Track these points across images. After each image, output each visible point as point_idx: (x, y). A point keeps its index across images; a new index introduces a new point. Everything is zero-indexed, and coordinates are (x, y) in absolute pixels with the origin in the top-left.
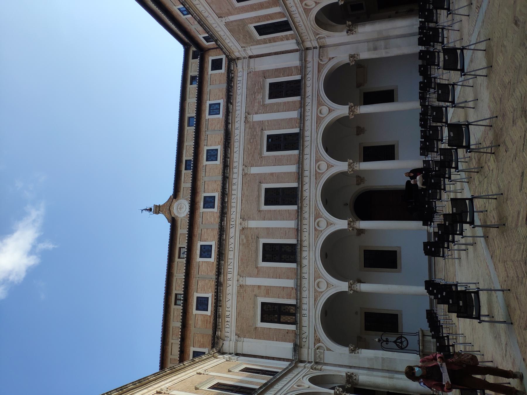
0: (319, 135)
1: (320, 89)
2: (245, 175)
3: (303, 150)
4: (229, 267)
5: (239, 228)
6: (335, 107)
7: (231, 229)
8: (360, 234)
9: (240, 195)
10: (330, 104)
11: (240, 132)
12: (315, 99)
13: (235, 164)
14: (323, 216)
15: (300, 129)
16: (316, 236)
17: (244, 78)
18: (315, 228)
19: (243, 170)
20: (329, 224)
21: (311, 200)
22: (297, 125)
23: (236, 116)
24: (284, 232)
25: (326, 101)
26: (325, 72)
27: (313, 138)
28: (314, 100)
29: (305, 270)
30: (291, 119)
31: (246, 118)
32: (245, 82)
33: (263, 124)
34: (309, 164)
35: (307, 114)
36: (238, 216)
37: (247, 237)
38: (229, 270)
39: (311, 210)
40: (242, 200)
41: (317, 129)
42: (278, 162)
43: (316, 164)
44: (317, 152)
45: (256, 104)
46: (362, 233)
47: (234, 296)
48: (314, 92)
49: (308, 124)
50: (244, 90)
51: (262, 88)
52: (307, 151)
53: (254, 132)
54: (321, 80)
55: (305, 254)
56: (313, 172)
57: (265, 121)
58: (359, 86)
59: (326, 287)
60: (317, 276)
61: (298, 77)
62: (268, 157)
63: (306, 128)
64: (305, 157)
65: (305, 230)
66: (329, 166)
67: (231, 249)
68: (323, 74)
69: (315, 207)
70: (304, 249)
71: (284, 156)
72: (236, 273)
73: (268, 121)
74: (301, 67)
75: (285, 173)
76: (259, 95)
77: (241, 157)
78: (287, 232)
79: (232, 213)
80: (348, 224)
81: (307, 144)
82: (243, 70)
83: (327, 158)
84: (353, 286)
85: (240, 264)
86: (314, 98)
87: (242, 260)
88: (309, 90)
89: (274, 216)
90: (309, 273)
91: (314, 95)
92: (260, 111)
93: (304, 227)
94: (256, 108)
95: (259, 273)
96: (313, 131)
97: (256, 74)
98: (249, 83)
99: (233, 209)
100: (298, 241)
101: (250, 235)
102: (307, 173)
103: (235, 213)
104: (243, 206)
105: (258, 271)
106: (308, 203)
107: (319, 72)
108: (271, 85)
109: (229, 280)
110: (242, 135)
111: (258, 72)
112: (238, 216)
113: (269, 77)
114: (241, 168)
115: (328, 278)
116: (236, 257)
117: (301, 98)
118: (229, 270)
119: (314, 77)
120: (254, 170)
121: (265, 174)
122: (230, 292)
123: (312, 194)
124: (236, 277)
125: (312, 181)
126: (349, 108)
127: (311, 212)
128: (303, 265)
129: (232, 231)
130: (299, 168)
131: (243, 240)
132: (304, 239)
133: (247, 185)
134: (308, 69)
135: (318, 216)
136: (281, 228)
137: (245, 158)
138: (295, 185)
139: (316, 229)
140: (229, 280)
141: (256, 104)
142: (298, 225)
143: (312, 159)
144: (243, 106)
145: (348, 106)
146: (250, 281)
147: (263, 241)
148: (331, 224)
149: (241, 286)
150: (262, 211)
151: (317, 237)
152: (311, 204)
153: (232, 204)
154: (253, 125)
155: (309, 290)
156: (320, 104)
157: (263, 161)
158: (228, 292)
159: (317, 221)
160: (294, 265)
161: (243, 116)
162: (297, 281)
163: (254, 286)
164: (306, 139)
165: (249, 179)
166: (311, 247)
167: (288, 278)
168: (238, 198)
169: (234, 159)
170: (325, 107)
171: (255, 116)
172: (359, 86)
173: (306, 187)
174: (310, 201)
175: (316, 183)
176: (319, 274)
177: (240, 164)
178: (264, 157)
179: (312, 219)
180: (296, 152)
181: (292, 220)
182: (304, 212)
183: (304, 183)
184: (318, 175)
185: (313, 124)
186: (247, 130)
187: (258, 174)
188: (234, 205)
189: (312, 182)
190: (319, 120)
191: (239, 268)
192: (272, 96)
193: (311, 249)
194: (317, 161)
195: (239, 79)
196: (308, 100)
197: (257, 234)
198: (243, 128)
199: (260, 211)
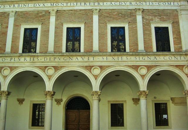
0: (122, 67)
1: (162, 68)
2: (91, 11)
3: (110, 55)
4: (23, 5)
5: (50, 9)
6: (146, 80)
7: (50, 4)
8: (56, 101)
9: (76, 8)
10: (148, 75)
11: (127, 6)
12: (154, 64)
13: (101, 4)
14: (56, 72)
15: (128, 53)
16: (41, 68)
17: (172, 7)
18: (47, 67)
19: (96, 10)
20: (50, 77)
21: (69, 63)
22: (132, 50)
23: (142, 2)
24: (45, 44)
25: (151, 72)
26: (177, 71)
27: (120, 63)
28: (152, 63)
29: (17, 59)
30: (137, 45)
31: (139, 9)
32: (169, 8)
33: (134, 23)
34: (100, 60)
35: (141, 57)
36: (60, 9)
37: (43, 16)
38: (21, 5)
39: (61, 63)
40: (72, 10)
41: (128, 66)
42: (102, 36)
43: (98, 66)
44: (109, 66)
45: (151, 17)
46: (57, 103)
47: (3, 10)
48: (159, 63)
49: (133, 58)
50: (163, 7)
51: (164, 21)
52: (110, 58)
53: (128, 16)
54: (169, 68)
55: (28, 59)
56: (91, 64)
57: (136, 25)
58: (172, 99)
59: (4, 75)
60: (12, 69)
61: (172, 49)
62: (106, 29)
63: (129, 57)
64: (105, 58)
65: (46, 59)
66: (96, 77)
67: (35, 5)
68: (174, 69)
69: (64, 67)
70: (32, 58)
71: (107, 41)
72: (18, 10)
73: (136, 27)
74: (181, 51)
75: (92, 42)
76: (158, 19)
77: (107, 7)
78: (45, 46)
79: (63, 3)
80: (49, 92)
81: (116, 58)
82: (180, 6)
83: (103, 74)
84: (5, 94)
85: (24, 12)
86: (154, 63)
87: (27, 13)
88: (162, 58)
89: (58, 35)
90: (14, 63)
91: (157, 63)
92: (145, 21)
93: (48, 58)
94: (147, 17)
95: (17, 26)
96: (126, 63)
97: (177, 16)
98: (169, 11)
99: (65, 4)
100: (37, 53)
101: (44, 18)
102: (91, 59)
103: (62, 5)
104: (67, 11)
105: (17, 26)
106: (67, 61)
107: (177, 66)
108: (167, 28)
109: (14, 6)
110: (125, 8)
111: (178, 18)
112: (59, 8)
113: (173, 27)
114: (98, 8)
115: (10, 76)
116: (29, 9)
117: (154, 53)
118: (21, 5)
119: (172, 63)
120: (96, 18)
121: (92, 27)
122: (6, 7)
123: (75, 64)
124: (14, 10)
125: (85, 63)
126: (144, 91)
127: (59, 63)
128: (20, 58)
129: (49, 5)
130: (95, 53)
131: (41, 13)
132: (39, 58)
133: (84, 13)
134: (179, 57)
135: (56, 68)
136: (48, 41)
137: (106, 11)
138: (82, 50)
139: (46, 67)
140: (14, 6)
141: (151, 17)
142: (49, 53)
143: (103, 63)
144: (149, 7)
145: (146, 90)
146: (11, 21)
147: (39, 27)
148: (49, 79)
149: (9, 15)
150: (63, 26)
151: (40, 68)
152: (66, 63)
153: (70, 3)
154: (133, 16)
155: (2, 63)
156: (149, 68)
157: (103, 25)
158: (6, 6)
159: (53, 68)
160: (20, 51)
161: (141, 7)
162: (8, 54)
163: (8, 23)
164: (120, 58)
165: (89, 14)
166: (33, 64)
167: (12, 47)
168: (73, 8)
169: (106, 3)
170: (147, 71)
171: (141, 17)
172: (172, 99)
173: (80, 59)
174: (68, 62)
175: (83, 67)
176: (13, 70)
177: (101, 7)
178: (106, 25)
179: (54, 64)
180: (109, 49)
181: (54, 49)
182: (60, 58)
183: (83, 57)
184: (89, 68)
185: (132, 63)
186: (129, 11)
187: (92, 21)
188: (69, 4)
189: (83, 63)
190: (136, 68)
191: (21, 12)
192: (157, 29)
193: (31, 64)
194: (101, 67)
195: (172, 3)
196: (152, 58)
197: (45, 23)
198: (131, 8)
199: (62, 24)
